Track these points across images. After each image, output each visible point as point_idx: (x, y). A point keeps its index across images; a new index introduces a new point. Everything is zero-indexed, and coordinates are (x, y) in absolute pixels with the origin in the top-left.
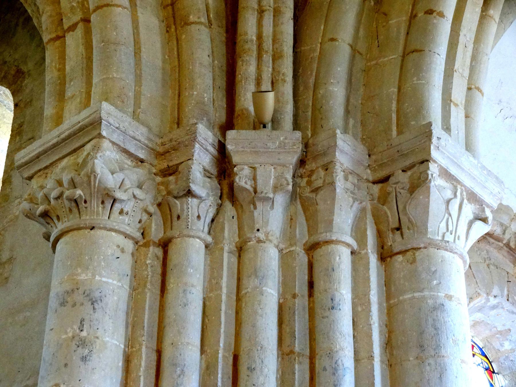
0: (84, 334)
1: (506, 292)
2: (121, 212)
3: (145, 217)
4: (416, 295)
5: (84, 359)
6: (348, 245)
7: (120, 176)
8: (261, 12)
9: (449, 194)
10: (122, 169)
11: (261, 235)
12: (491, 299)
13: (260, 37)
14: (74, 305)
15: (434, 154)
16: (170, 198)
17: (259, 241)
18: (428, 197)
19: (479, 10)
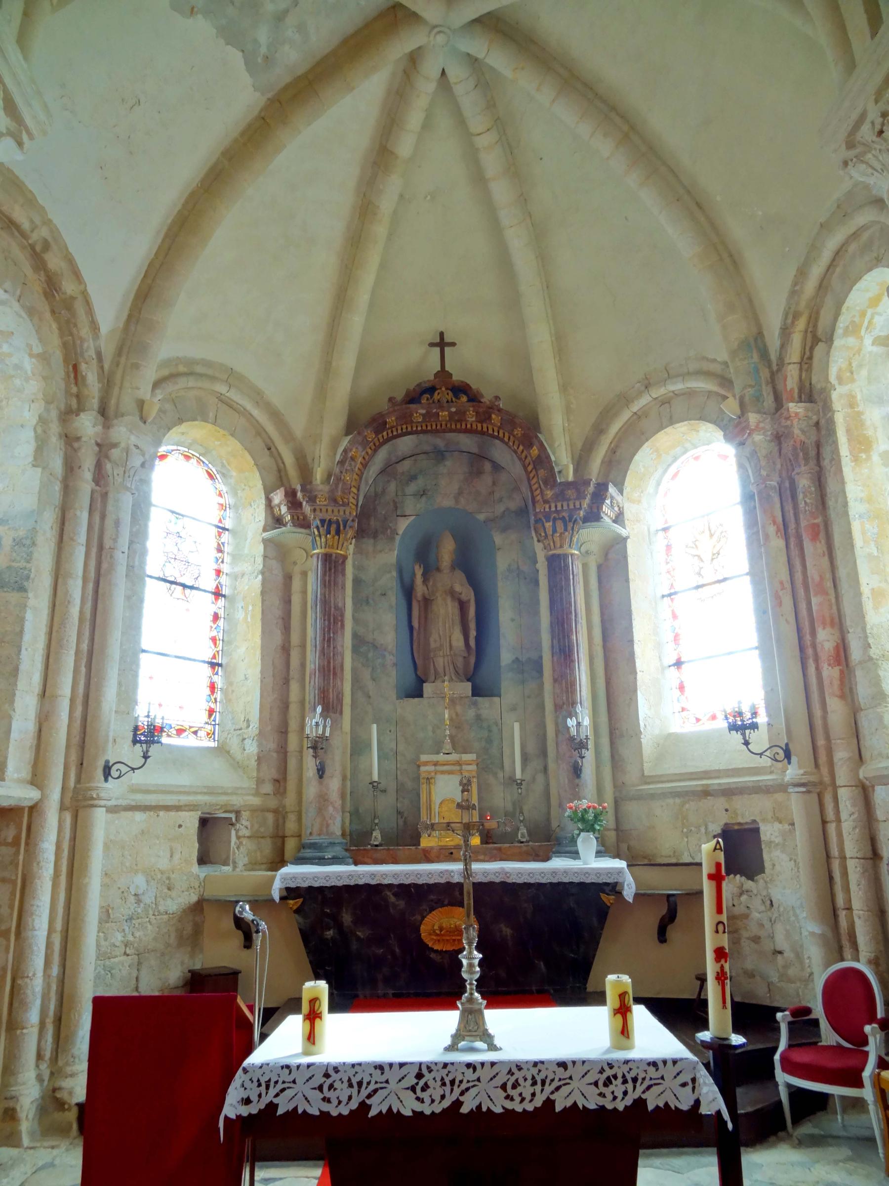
1: (18, 293)
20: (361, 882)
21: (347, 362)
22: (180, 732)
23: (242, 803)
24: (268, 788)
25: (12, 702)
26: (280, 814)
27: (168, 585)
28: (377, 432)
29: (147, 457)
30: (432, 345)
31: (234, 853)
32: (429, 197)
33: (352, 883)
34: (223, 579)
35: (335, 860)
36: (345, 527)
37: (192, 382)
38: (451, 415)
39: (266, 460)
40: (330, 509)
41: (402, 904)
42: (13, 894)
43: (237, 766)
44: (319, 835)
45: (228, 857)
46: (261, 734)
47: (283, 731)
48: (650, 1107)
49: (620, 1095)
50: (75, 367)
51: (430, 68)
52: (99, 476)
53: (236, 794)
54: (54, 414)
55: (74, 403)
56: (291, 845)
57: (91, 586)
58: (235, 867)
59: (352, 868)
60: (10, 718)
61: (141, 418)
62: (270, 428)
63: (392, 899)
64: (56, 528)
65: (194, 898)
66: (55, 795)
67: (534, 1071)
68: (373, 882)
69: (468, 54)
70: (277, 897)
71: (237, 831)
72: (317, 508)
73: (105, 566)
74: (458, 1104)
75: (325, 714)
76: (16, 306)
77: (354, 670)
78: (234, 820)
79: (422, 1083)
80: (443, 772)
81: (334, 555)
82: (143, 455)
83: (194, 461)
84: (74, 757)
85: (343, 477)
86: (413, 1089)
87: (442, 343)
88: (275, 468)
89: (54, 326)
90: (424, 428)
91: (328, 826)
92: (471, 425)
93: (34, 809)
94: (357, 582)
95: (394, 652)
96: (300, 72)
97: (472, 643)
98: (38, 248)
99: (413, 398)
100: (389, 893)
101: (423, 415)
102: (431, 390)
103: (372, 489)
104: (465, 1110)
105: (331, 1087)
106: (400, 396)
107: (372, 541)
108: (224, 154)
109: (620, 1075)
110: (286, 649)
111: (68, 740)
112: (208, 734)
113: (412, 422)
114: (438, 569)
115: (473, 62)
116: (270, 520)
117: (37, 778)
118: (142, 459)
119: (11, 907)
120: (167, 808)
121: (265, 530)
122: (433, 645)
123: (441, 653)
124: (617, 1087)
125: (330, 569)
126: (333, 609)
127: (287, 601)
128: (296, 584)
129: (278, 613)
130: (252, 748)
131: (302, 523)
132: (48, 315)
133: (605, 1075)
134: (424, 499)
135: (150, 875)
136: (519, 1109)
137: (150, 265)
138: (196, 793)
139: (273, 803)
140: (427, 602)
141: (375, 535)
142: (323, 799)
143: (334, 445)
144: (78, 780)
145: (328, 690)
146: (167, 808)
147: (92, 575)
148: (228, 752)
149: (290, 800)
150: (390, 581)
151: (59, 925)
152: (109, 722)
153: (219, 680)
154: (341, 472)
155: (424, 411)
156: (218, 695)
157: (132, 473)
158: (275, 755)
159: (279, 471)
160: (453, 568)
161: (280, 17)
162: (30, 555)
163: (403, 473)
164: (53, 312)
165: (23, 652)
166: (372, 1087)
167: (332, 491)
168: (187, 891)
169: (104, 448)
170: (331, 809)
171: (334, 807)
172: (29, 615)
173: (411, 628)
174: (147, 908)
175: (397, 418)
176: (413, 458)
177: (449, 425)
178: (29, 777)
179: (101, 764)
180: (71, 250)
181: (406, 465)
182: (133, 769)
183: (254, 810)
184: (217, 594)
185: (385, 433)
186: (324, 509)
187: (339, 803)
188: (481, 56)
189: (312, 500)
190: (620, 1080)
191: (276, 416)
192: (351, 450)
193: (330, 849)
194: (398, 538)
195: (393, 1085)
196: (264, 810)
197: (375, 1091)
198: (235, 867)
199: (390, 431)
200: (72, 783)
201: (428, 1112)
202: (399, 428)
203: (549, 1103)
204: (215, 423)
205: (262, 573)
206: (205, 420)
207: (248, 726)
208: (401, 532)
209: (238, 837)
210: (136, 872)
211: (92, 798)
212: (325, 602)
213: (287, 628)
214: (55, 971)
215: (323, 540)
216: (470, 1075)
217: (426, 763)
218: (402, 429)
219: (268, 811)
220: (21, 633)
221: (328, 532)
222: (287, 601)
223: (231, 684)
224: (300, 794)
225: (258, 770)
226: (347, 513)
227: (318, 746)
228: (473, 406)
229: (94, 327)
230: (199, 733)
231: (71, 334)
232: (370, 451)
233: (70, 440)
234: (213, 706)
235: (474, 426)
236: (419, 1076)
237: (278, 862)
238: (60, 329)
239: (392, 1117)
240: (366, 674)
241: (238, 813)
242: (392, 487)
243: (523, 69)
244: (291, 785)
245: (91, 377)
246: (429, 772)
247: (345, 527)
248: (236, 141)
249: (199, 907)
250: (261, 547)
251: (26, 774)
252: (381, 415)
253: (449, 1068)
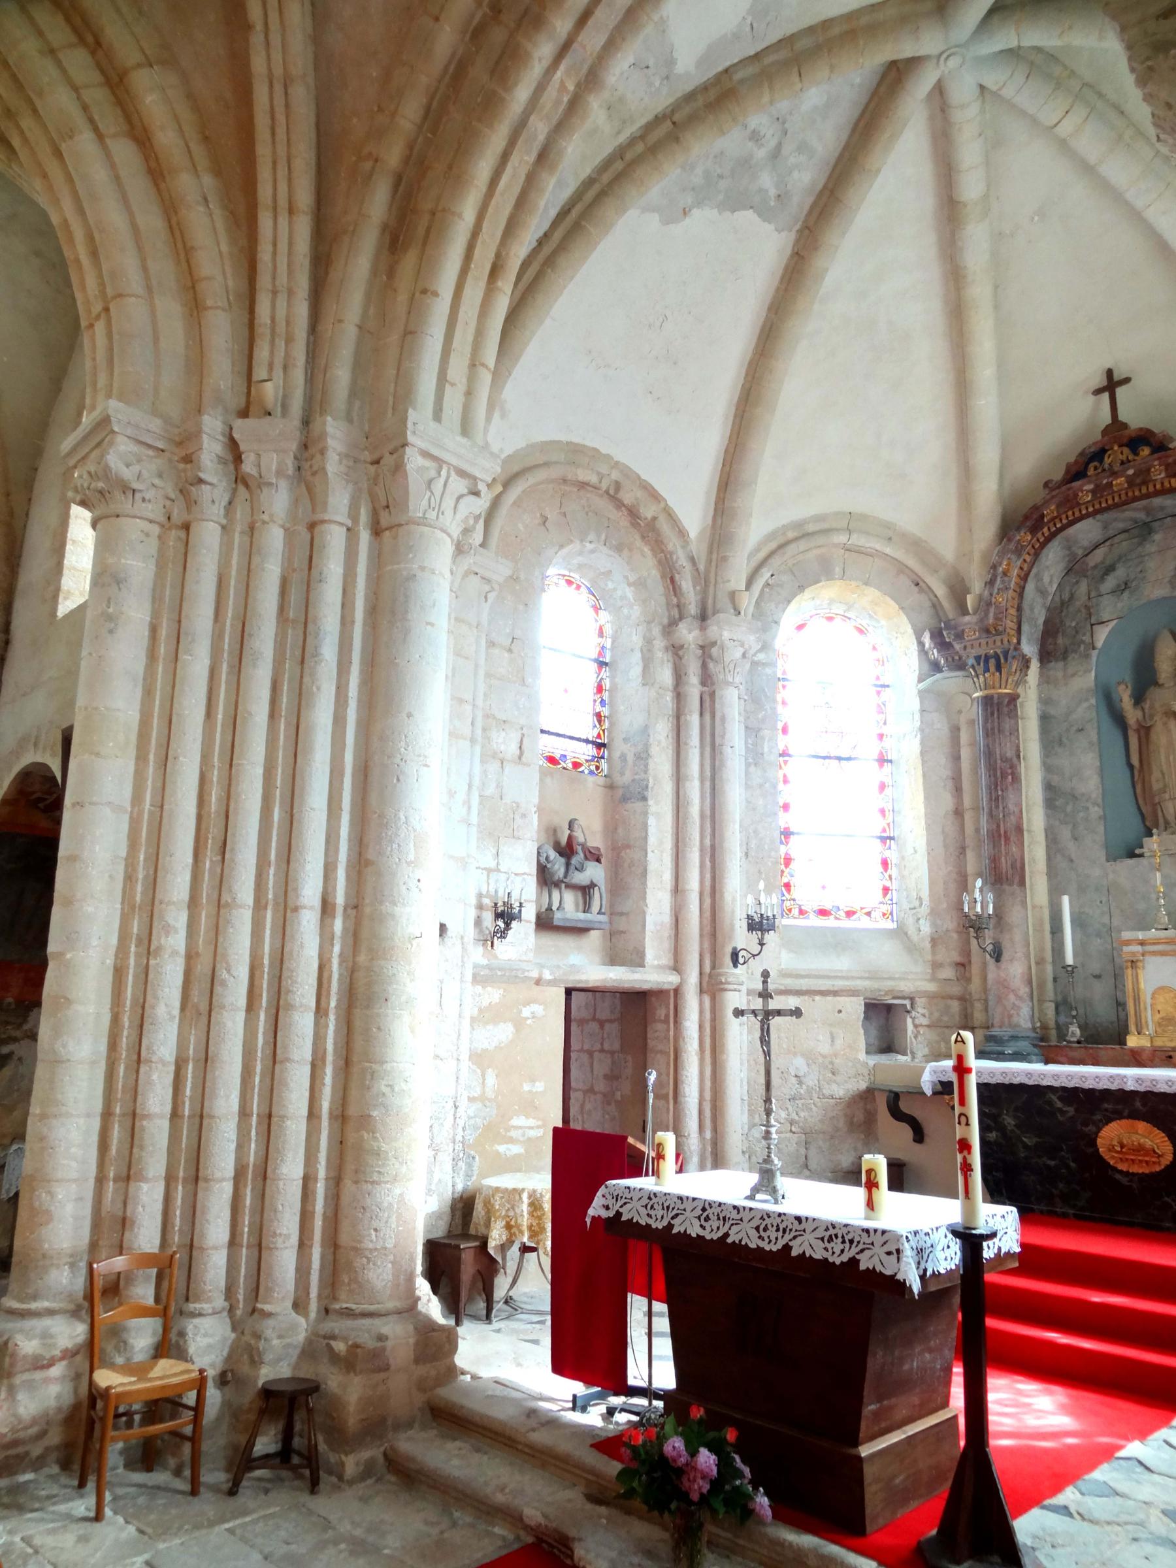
0: (111, 610)
1: (603, 537)
2: (144, 500)
3: (168, 503)
4: (396, 567)
5: (111, 632)
6: (342, 524)
7: (136, 468)
8: (275, 293)
9: (433, 473)
10: (139, 461)
11: (265, 517)
12: (588, 544)
13: (273, 319)
14: (103, 585)
15: (411, 438)
16: (188, 486)
17: (264, 522)
18: (407, 478)
19: (483, 284)
20: (1016, 1081)
21: (987, 456)
22: (850, 914)
23: (912, 989)
24: (948, 973)
25: (644, 898)
27: (822, 761)
28: (1034, 530)
29: (747, 646)
30: (1098, 392)
31: (911, 1043)
32: (1036, 218)
33: (1007, 1081)
34: (887, 743)
35: (1018, 1056)
36: (1006, 659)
37: (802, 545)
38: (1131, 482)
39: (915, 597)
40: (983, 641)
41: (1071, 1110)
42: (668, 1064)
43: (911, 948)
44: (1001, 1027)
45: (906, 1048)
46: (934, 913)
48: (862, 1267)
49: (838, 1252)
50: (672, 580)
51: (963, 91)
52: (706, 679)
53: (904, 979)
54: (656, 631)
55: (675, 612)
57: (708, 784)
58: (913, 1058)
59: (1039, 1067)
60: (644, 913)
61: (735, 609)
63: (1059, 1104)
64: (673, 735)
65: (863, 1086)
66: (693, 979)
67: (779, 1220)
68: (1030, 1082)
69: (1002, 51)
70: (928, 1092)
71: (913, 1019)
72: (968, 644)
73: (717, 763)
74: (727, 1235)
76: (605, 550)
78: (909, 1007)
79: (705, 1214)
80: (1154, 953)
81: (996, 697)
82: (742, 645)
83: (838, 620)
84: (706, 945)
85: (993, 600)
86: (699, 1218)
87: (1111, 384)
88: (928, 604)
89: (646, 550)
90: (1097, 506)
91: (1010, 1016)
92: (1162, 484)
93: (677, 991)
95: (1100, 801)
96: (820, 186)
98: (612, 492)
99: (1076, 473)
100: (1054, 1098)
101: (1093, 492)
102: (1098, 455)
103: (1057, 599)
104: (729, 1240)
105: (652, 1207)
106: (1058, 475)
107: (1061, 664)
108: (769, 309)
109: (840, 1235)
111: (701, 929)
112: (884, 915)
113: (1079, 504)
114: (1156, 684)
115: (1013, 54)
116: (926, 667)
117: (677, 966)
118: (742, 650)
119: (668, 1075)
120: (823, 993)
121: (920, 680)
122: (1156, 787)
123: (1167, 796)
124: (837, 1246)
125: (992, 714)
126: (999, 761)
129: (946, 772)
130: (926, 928)
132: (639, 543)
133: (828, 1234)
134: (1126, 594)
135: (810, 1058)
136: (767, 1248)
137: (726, 451)
138: (853, 978)
139: (956, 990)
140: (1145, 731)
141: (1065, 656)
144: (713, 967)
145: (1000, 859)
146: (823, 993)
147: (708, 773)
148: (906, 934)
149: (975, 985)
150: (1088, 711)
151: (708, 1095)
152: (733, 912)
153: (893, 856)
154: (991, 595)
155: (1091, 487)
156: (893, 871)
157: (731, 667)
158: (955, 936)
159: (934, 606)
161: (776, 154)
162: (646, 766)
163: (1095, 567)
164: (643, 537)
165: (650, 855)
166: (675, 1212)
167: (981, 620)
168: (855, 1077)
169: (706, 650)
170: (1012, 997)
171: (1016, 995)
172: (652, 821)
173: (1131, 767)
174: (809, 1091)
175: (1058, 506)
176: (1108, 543)
177: (1130, 494)
178: (671, 963)
179: (729, 950)
180: (643, 477)
181: (1099, 554)
182: (754, 956)
183: (932, 997)
184: (882, 760)
185: (1045, 530)
186: (976, 643)
187: (1024, 990)
188: (1014, 43)
190: (840, 1240)
191: (916, 545)
192: (1000, 564)
193: (1012, 1043)
194: (1095, 653)
195: (687, 1214)
197: (677, 1215)
198: (913, 1058)
199: (1051, 525)
200: (707, 969)
201: (708, 1237)
202: (1064, 516)
203: (787, 1248)
205: (921, 730)
207: (921, 905)
208: (1099, 644)
209: (916, 1026)
210: (795, 1054)
211: (722, 983)
214: (708, 1134)
215: (982, 679)
216: (734, 1215)
217: (1128, 943)
218: (1067, 517)
219: (951, 998)
220: (646, 838)
221: (987, 670)
223: (903, 858)
224: (984, 979)
225: (934, 953)
226: (1005, 641)
228: (1159, 458)
229: (682, 533)
230: (873, 915)
231: (662, 551)
232: (1028, 558)
233: (676, 650)
234: (888, 884)
235: (1167, 485)
236: (704, 1210)
238: (652, 550)
239: (685, 1235)
240: (1065, 833)
242: (1083, 587)
243: (1070, 28)
245: (686, 584)
246: (1133, 954)
247: (1006, 659)
248: (777, 290)
249: (868, 1095)
251: (667, 960)
252: (1035, 508)
253: (723, 1207)
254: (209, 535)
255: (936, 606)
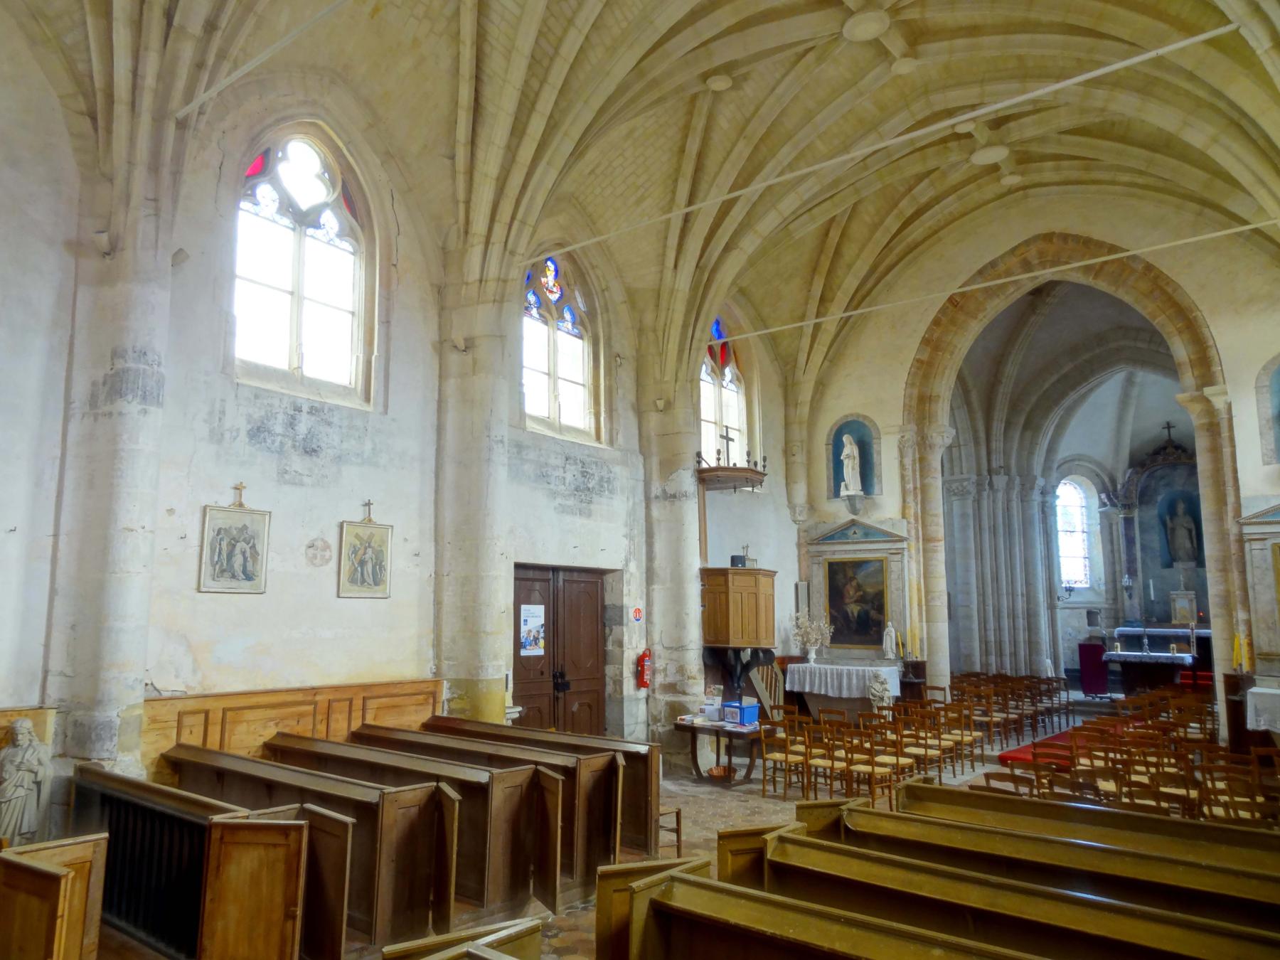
22: (1076, 582)
24: (1111, 602)
26: (1116, 611)
43: (1098, 594)
46: (1106, 583)
47: (1114, 581)
56: (1121, 621)
62: (1098, 471)
70: (1116, 636)
75: (1129, 578)
77: (1142, 558)
87: (1169, 426)
94: (1141, 524)
97: (1195, 545)
102: (1165, 448)
110: (1112, 551)
121: (1100, 508)
127: (1111, 534)
128: (1114, 527)
130: (1103, 588)
131: (1114, 505)
140: (1173, 530)
142: (1132, 606)
143: (1125, 473)
149: (1119, 605)
150: (1155, 522)
160: (1185, 514)
183: (1106, 609)
187: (1138, 607)
189: (1117, 498)
191: (1099, 464)
196: (1111, 609)
204: (1076, 474)
206: (1071, 474)
212: (1126, 535)
213: (1112, 542)
222: (1111, 534)
224: (1123, 604)
227: (1128, 588)
237: (1117, 625)
241: (1100, 610)
244: (1119, 600)
250: (1098, 515)
254: (985, 503)
255: (1103, 483)
